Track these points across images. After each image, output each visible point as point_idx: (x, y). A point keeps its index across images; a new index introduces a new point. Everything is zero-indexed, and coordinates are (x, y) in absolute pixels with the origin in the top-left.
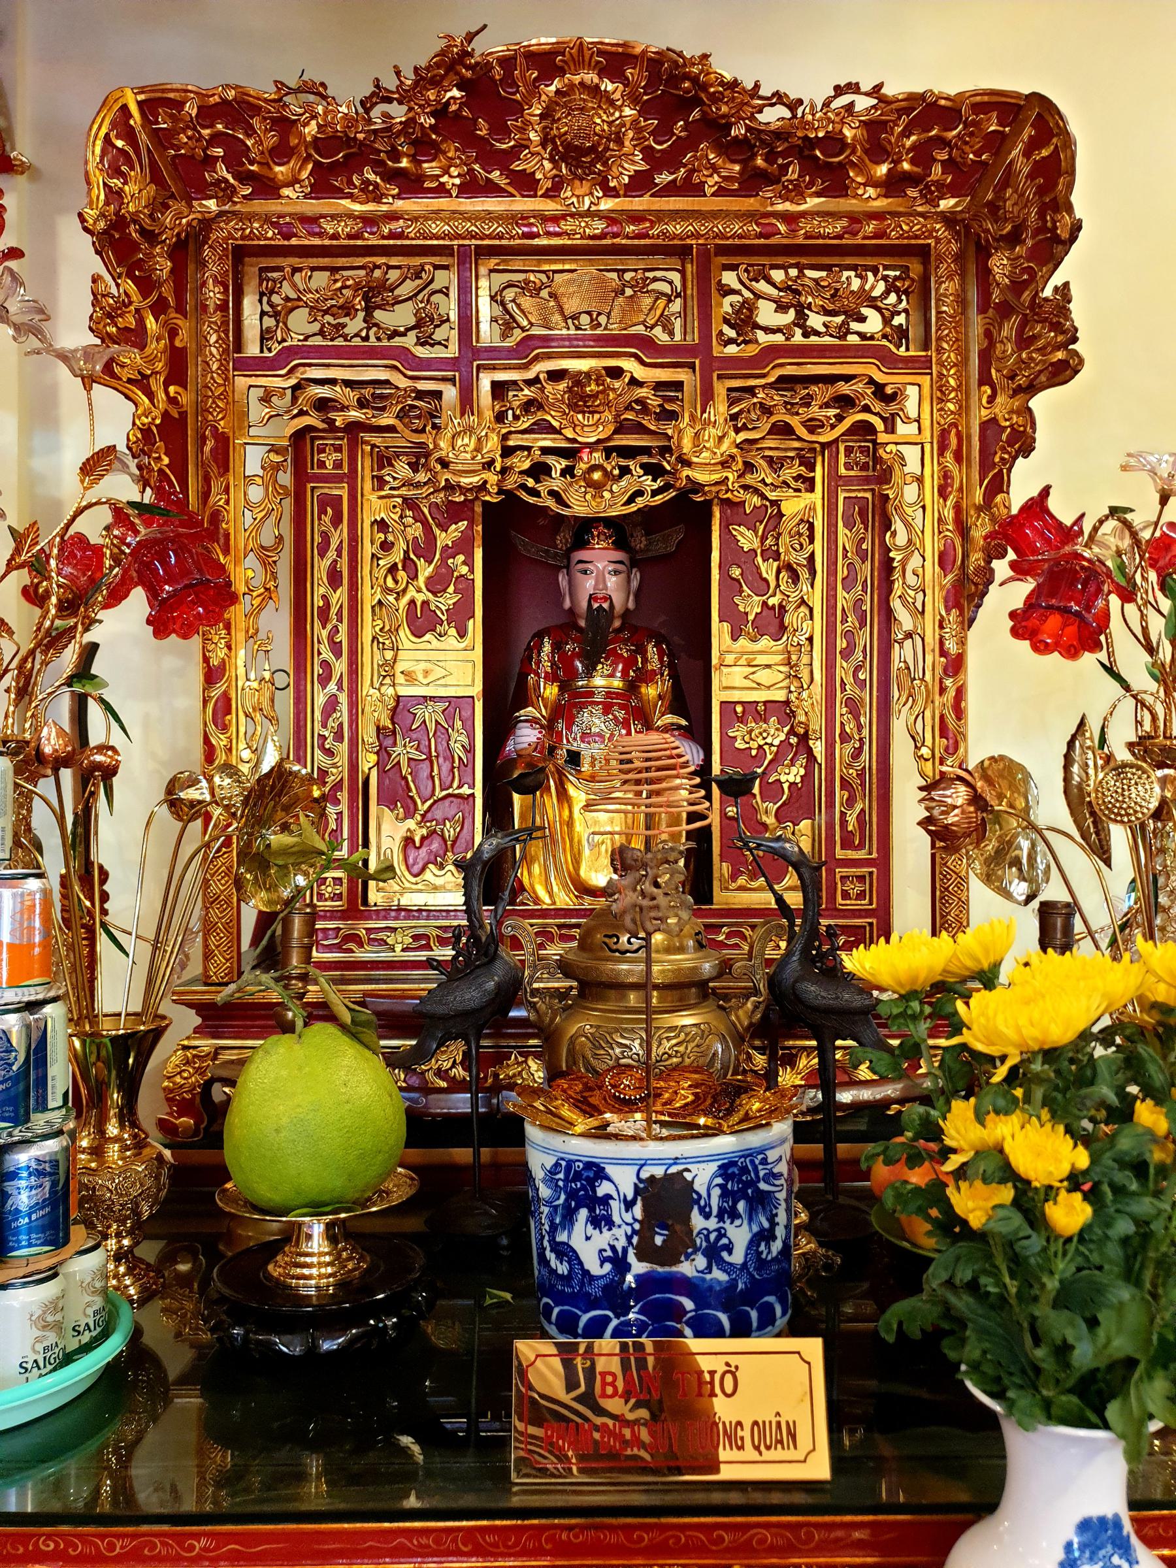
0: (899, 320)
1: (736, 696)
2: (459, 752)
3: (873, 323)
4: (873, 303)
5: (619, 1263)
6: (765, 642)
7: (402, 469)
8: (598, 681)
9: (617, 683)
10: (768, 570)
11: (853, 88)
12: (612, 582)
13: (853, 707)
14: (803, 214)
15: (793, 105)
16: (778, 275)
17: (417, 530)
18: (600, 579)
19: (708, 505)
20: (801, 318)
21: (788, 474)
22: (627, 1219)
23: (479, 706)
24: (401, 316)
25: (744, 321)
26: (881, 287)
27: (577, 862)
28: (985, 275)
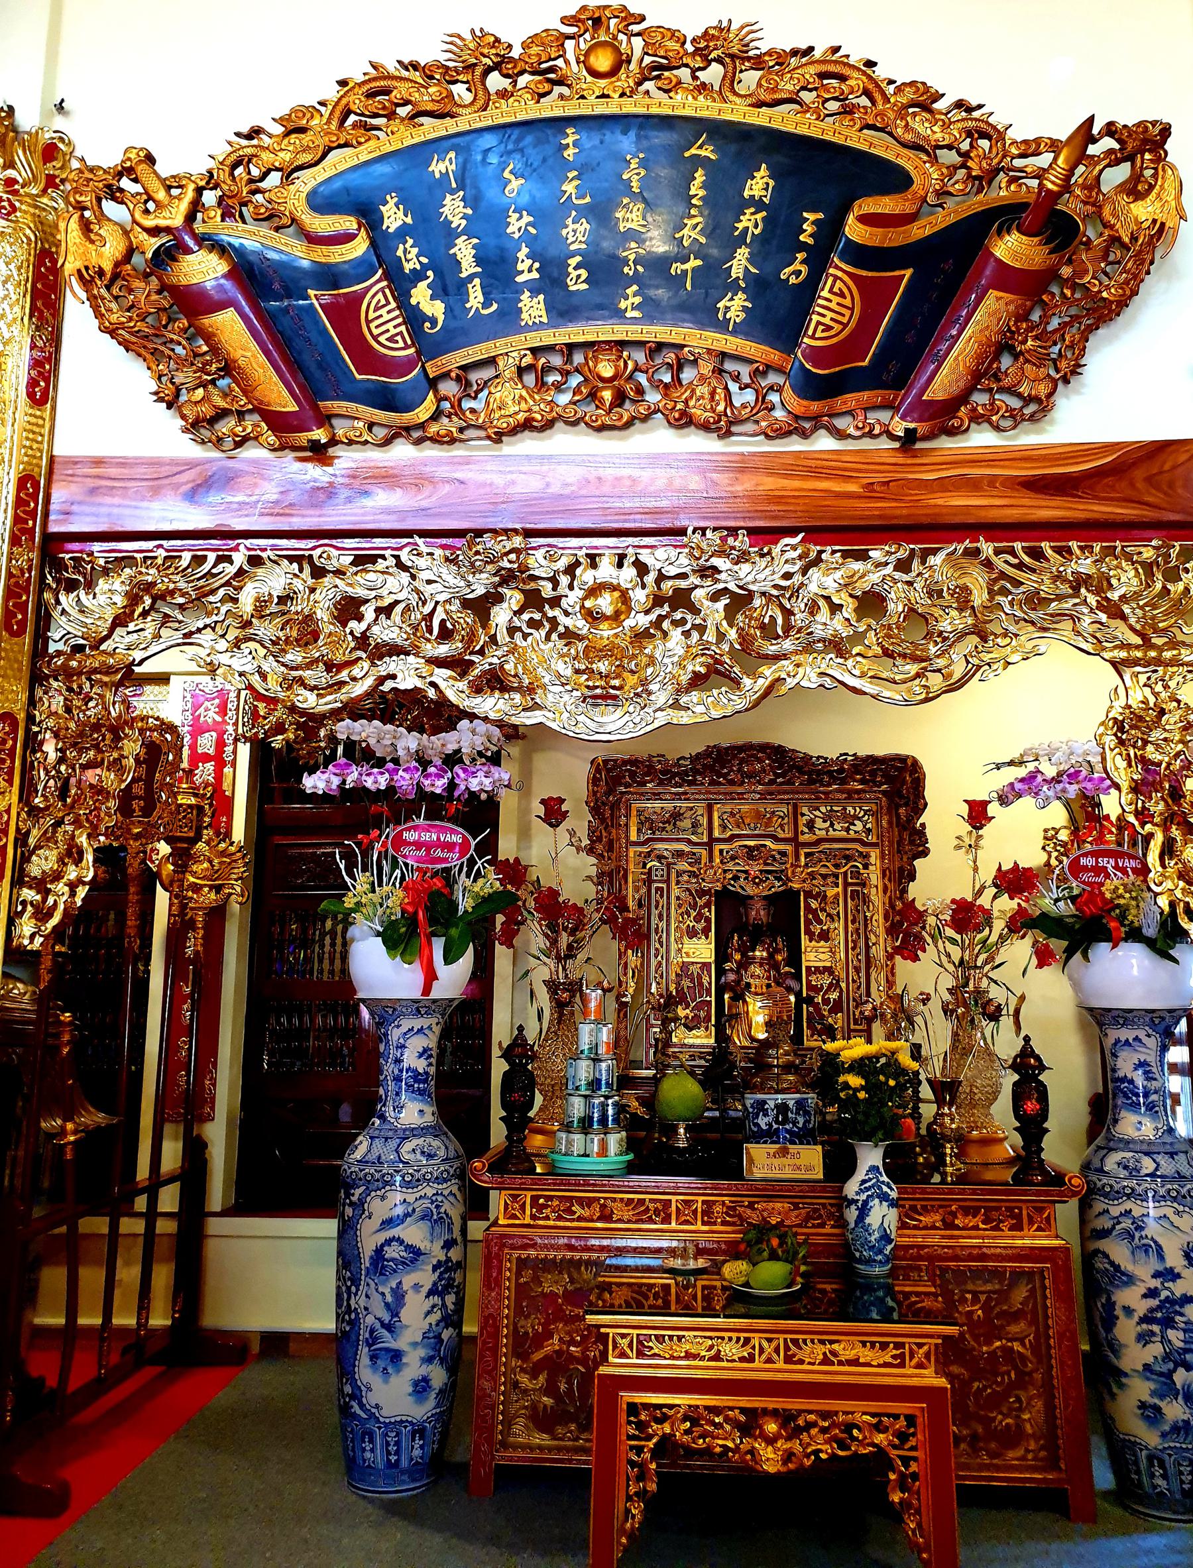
0: (869, 826)
1: (811, 964)
2: (706, 984)
3: (859, 826)
4: (859, 819)
5: (770, 1125)
6: (822, 943)
7: (686, 878)
8: (757, 953)
9: (765, 954)
10: (822, 916)
11: (846, 754)
12: (762, 913)
13: (857, 969)
14: (831, 792)
15: (826, 759)
16: (823, 809)
17: (690, 899)
18: (758, 912)
19: (798, 892)
20: (832, 825)
21: (829, 880)
22: (772, 1114)
23: (713, 966)
24: (686, 824)
25: (811, 825)
26: (862, 813)
27: (750, 1028)
28: (898, 816)
